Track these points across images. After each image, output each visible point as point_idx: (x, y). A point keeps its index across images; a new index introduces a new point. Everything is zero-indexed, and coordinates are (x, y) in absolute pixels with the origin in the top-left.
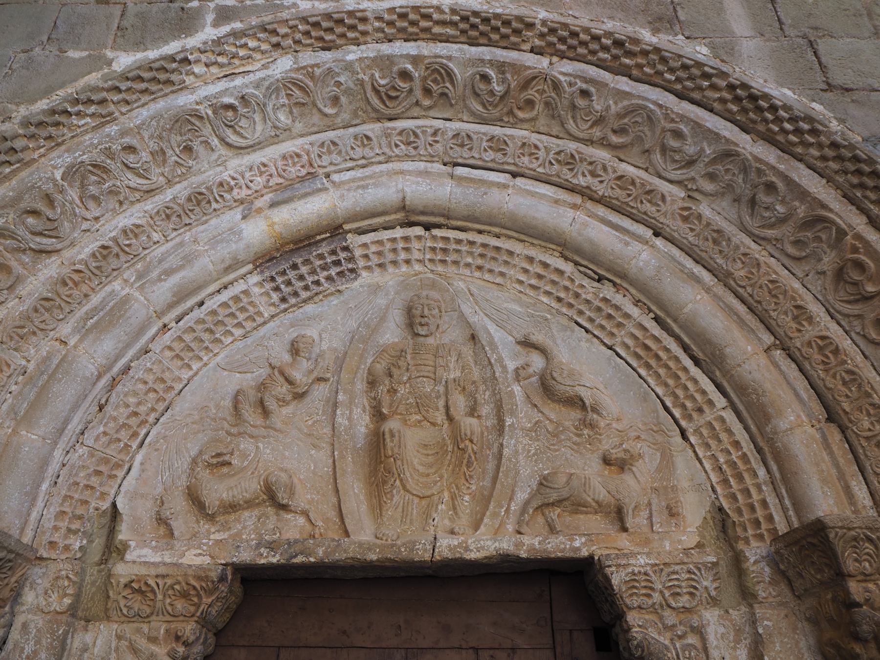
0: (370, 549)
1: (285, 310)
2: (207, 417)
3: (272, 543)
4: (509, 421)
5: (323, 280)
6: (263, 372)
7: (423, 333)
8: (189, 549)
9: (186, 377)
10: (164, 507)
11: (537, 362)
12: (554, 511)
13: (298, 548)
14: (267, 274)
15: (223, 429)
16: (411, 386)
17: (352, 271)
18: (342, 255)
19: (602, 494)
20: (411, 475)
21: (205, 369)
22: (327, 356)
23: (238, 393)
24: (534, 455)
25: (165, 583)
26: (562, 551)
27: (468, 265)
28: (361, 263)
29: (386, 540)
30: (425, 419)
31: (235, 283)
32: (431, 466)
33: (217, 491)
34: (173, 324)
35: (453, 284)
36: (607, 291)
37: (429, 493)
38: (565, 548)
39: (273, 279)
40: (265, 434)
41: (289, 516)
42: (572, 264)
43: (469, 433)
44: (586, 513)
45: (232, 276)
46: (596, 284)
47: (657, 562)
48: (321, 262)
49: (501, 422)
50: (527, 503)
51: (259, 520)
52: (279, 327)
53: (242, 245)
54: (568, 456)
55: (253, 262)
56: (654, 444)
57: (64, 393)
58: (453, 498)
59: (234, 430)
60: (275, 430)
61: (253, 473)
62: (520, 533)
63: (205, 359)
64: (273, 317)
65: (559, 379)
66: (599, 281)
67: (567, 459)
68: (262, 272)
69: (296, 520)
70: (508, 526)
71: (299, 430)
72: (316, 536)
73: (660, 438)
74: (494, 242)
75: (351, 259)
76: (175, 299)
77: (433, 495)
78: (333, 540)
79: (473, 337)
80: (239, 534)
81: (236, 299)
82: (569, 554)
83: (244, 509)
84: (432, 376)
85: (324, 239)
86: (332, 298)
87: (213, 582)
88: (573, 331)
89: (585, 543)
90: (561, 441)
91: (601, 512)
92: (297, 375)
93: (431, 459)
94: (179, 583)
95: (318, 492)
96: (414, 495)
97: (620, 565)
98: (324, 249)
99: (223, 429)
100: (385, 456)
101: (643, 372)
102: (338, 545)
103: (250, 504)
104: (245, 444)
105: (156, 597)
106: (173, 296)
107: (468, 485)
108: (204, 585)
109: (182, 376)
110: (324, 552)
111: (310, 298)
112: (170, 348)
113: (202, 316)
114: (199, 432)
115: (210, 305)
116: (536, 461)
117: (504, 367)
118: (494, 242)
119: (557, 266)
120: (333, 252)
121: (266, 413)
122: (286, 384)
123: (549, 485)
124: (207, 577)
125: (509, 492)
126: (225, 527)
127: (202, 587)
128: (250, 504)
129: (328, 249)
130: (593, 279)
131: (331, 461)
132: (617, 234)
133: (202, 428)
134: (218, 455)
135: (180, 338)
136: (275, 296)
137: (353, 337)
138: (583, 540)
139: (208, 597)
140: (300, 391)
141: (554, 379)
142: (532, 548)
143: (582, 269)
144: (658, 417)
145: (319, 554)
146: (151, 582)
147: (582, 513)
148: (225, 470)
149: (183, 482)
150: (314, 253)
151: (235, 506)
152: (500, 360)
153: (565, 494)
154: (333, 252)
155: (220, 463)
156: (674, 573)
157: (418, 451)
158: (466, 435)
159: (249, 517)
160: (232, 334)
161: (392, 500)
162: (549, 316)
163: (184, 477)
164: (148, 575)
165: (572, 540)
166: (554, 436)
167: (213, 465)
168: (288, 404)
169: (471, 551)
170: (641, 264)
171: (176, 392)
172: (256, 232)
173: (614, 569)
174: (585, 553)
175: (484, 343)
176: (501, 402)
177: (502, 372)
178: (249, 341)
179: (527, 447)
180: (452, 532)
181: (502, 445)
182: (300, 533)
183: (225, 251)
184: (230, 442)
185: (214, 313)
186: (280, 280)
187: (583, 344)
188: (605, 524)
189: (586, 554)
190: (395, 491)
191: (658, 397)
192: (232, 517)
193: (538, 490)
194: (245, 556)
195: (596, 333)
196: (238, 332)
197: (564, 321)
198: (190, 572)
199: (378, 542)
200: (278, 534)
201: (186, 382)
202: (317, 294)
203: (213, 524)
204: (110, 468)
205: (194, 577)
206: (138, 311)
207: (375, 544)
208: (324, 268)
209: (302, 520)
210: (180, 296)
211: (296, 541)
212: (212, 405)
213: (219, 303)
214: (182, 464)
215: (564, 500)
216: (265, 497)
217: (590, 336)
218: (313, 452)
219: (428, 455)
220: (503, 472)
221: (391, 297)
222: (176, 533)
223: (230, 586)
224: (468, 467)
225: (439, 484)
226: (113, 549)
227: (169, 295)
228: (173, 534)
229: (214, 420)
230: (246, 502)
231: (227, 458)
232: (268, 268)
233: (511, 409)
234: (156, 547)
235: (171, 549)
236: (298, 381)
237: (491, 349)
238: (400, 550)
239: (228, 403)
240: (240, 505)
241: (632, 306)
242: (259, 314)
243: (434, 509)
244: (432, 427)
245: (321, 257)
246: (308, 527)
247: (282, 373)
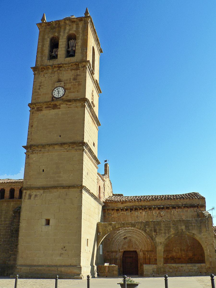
33: (123, 248)
57: (117, 245)
155: (123, 247)
172: (123, 238)
204: (119, 247)
206: (119, 241)
226: (119, 250)
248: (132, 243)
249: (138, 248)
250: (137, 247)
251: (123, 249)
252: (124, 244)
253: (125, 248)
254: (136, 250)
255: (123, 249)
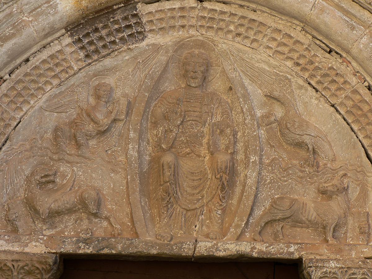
0: (152, 247)
1: (90, 64)
2: (36, 146)
3: (87, 240)
4: (253, 159)
5: (117, 41)
6: (73, 113)
7: (193, 85)
8: (31, 242)
9: (19, 116)
10: (10, 212)
11: (279, 112)
12: (279, 225)
13: (104, 244)
14: (76, 37)
15: (47, 155)
16: (183, 127)
17: (140, 33)
18: (133, 21)
19: (313, 216)
20: (182, 194)
21: (32, 111)
22: (121, 102)
23: (56, 129)
24: (269, 183)
25: (19, 265)
26: (281, 254)
27: (230, 32)
28: (148, 28)
29: (164, 241)
30: (193, 151)
31: (52, 44)
32: (195, 188)
33: (47, 202)
34: (7, 76)
35: (218, 46)
36: (333, 61)
37: (194, 207)
38: (284, 252)
39: (80, 40)
40: (78, 161)
41: (96, 220)
42: (310, 37)
43: (224, 168)
44: (302, 227)
45: (49, 39)
46: (327, 55)
47: (343, 266)
48: (116, 26)
49: (247, 157)
50: (262, 217)
51: (76, 222)
52: (85, 77)
53: (57, 17)
54: (294, 185)
55: (66, 28)
56: (356, 181)
58: (210, 211)
59: (55, 157)
60: (85, 158)
61: (70, 189)
62: (255, 240)
63: (32, 102)
64: (80, 69)
65: (292, 129)
66: (330, 52)
67: (292, 188)
68: (72, 35)
69: (101, 223)
70: (247, 234)
71: (102, 158)
72: (116, 235)
73: (360, 177)
74: (252, 16)
75: (138, 24)
76: (9, 59)
77: (196, 208)
78: (128, 239)
79: (231, 89)
80: (62, 232)
81: (52, 57)
82: (287, 257)
83: (65, 214)
84: (198, 119)
85: (119, 8)
86: (124, 54)
87: (50, 265)
88: (307, 90)
89: (297, 249)
90: (289, 175)
91: (311, 227)
92: (100, 116)
93: (196, 183)
94: (27, 265)
95: (116, 204)
96: (183, 208)
97: (318, 266)
98: (119, 16)
99: (47, 155)
100: (164, 182)
101: (355, 128)
102: (132, 243)
103: (70, 211)
104: (63, 168)
105: (12, 274)
106: (8, 58)
107: (221, 203)
108: (44, 267)
109: (16, 116)
110: (122, 247)
111: (109, 54)
112: (6, 95)
113: (28, 70)
114: (30, 157)
115: (34, 62)
116: (270, 188)
117: (253, 116)
118: (252, 16)
119: (299, 39)
120: (126, 18)
121: (78, 146)
122: (92, 123)
123: (277, 207)
124: (46, 262)
125: (249, 210)
126: (53, 226)
127: (43, 268)
128: (70, 211)
129: (122, 16)
130: (326, 51)
131: (125, 182)
132: (347, 19)
133: (33, 155)
134: (46, 176)
135: (13, 88)
136: (82, 54)
137: (141, 86)
138: (296, 247)
139: (46, 274)
140: (102, 129)
141: (288, 129)
142: (260, 252)
143: (318, 42)
144: (361, 161)
145: (118, 248)
146: (9, 264)
147: (299, 227)
148: (51, 186)
149: (21, 194)
150: (112, 20)
151: (60, 213)
152: (251, 110)
153: (288, 214)
154: (126, 18)
155: (47, 182)
156: (353, 274)
157: (187, 177)
158: (221, 169)
159: (69, 222)
160: (51, 84)
161: (167, 211)
162: (289, 77)
163: (21, 190)
164: (7, 260)
165: (288, 247)
166: (285, 171)
167: (42, 183)
168: (93, 138)
169: (220, 251)
170: (362, 46)
171: (12, 128)
173: (313, 268)
174: (296, 256)
175: (239, 95)
176: (248, 143)
177: (251, 120)
178: (63, 88)
179: (265, 177)
180: (207, 236)
181: (246, 176)
182: (105, 232)
183: (44, 22)
184: (53, 166)
185: (36, 68)
186: (86, 41)
187: (313, 100)
188: (314, 235)
189: (298, 257)
190: (169, 206)
191: (363, 147)
192: (57, 219)
193: (269, 210)
194: (69, 248)
195: (323, 93)
196: (55, 82)
197: (301, 82)
198: (35, 259)
199: (158, 241)
200: (90, 233)
201: (18, 121)
202: (113, 51)
203: (44, 224)
205: (38, 262)
207: (156, 243)
208: (118, 31)
209: (105, 224)
210: (13, 56)
211: (103, 239)
212: (38, 137)
213: (40, 61)
214: (20, 181)
215: (287, 218)
216: (80, 207)
217: (318, 95)
218: (112, 175)
219: (194, 180)
220: (245, 196)
221: (169, 55)
222: (20, 230)
223: (59, 266)
224: (222, 191)
225: (201, 201)
227: (5, 57)
228: (18, 231)
229: (40, 148)
230: (67, 210)
231: (52, 178)
232: (76, 32)
233: (255, 149)
234: (8, 240)
235: (19, 241)
236: (101, 122)
237: (244, 101)
238: (173, 249)
239: (49, 135)
240: (63, 212)
241: (352, 76)
242: (70, 67)
243: (197, 219)
244: (197, 158)
245: (116, 22)
246: (110, 228)
247: (89, 115)
248: (219, 129)
249: (336, 207)
250: (307, 198)
251: (54, 216)
252: (71, 137)
253: (89, 207)
254: (292, 251)
255: (54, 216)
